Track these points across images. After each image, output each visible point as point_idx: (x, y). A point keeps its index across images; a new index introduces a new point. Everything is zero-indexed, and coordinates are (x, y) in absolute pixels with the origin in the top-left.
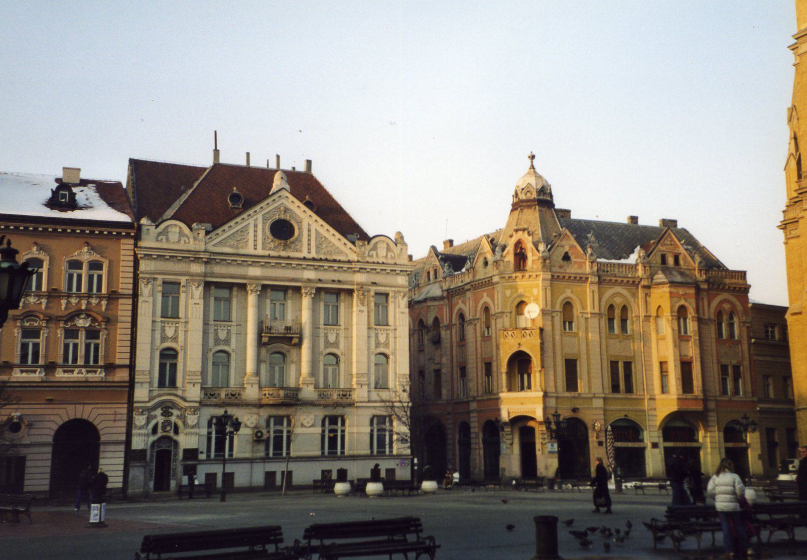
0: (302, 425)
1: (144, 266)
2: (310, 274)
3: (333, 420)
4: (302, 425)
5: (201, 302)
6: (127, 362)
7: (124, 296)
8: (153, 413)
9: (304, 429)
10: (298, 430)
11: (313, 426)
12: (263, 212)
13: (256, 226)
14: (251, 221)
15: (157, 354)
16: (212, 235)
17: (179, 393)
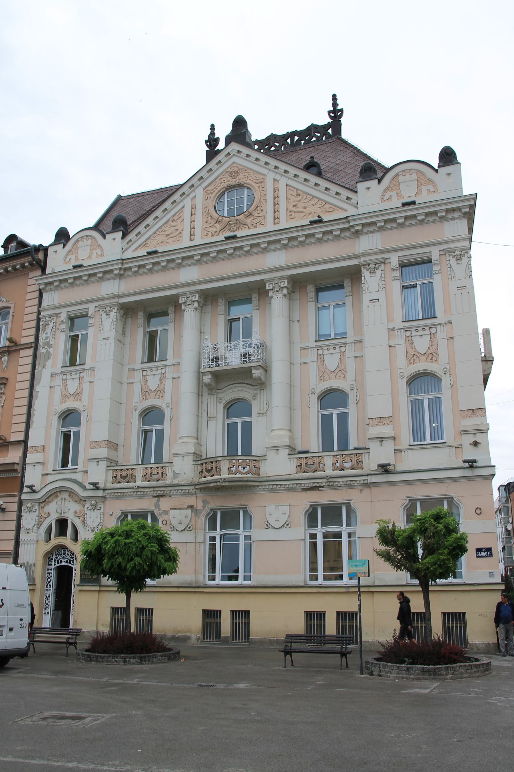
0: (269, 526)
1: (48, 299)
2: (276, 259)
3: (333, 513)
4: (269, 526)
5: (112, 334)
6: (21, 437)
7: (27, 346)
8: (47, 509)
9: (271, 530)
10: (257, 534)
11: (286, 525)
12: (204, 185)
13: (193, 207)
14: (187, 203)
15: (55, 419)
16: (132, 236)
17: (79, 477)
